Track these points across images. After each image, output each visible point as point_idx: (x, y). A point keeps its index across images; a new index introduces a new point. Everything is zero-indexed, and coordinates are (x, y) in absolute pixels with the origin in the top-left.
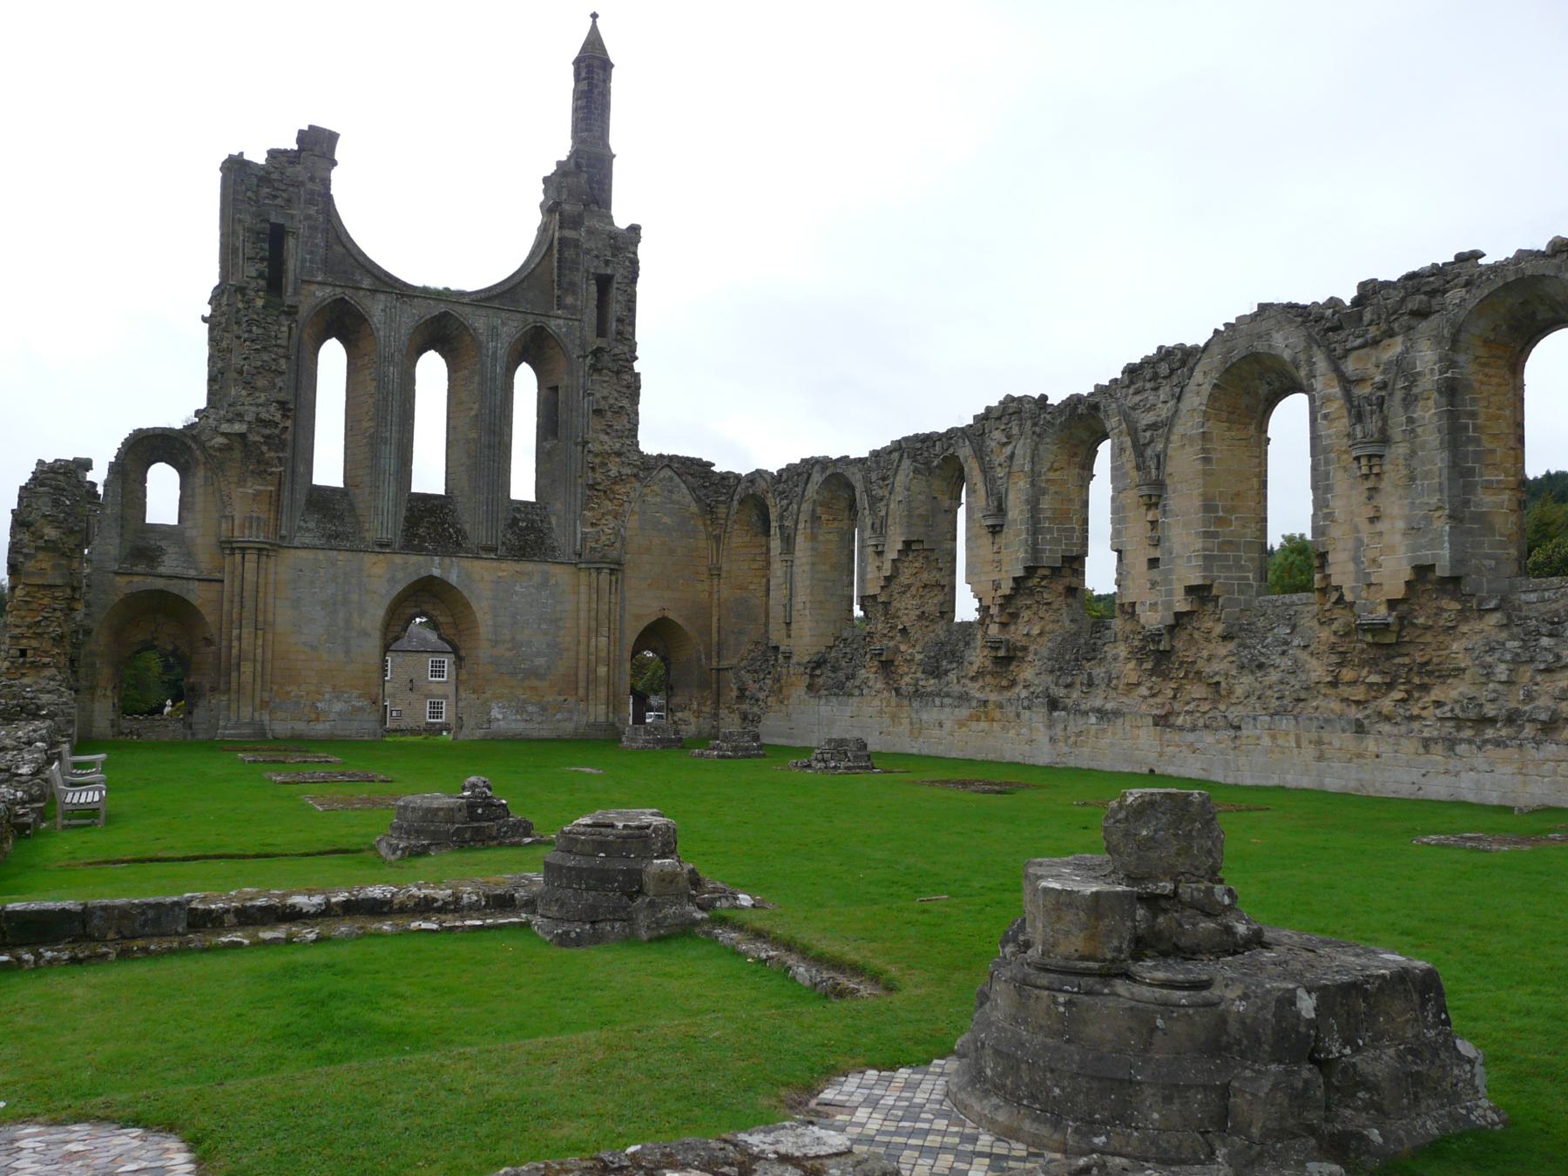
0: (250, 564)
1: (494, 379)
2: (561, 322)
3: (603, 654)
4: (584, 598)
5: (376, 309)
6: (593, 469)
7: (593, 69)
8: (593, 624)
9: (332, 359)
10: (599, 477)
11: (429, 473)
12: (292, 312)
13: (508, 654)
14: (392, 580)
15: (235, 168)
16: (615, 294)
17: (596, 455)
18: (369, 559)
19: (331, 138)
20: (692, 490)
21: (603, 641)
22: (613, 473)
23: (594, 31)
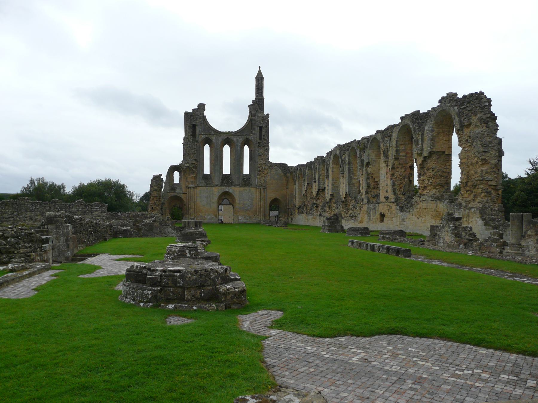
0: (192, 190)
5: (214, 138)
7: (260, 79)
9: (207, 149)
10: (260, 169)
11: (227, 170)
12: (197, 142)
14: (219, 192)
15: (186, 114)
16: (263, 130)
18: (214, 188)
19: (204, 105)
20: (282, 170)
23: (260, 70)
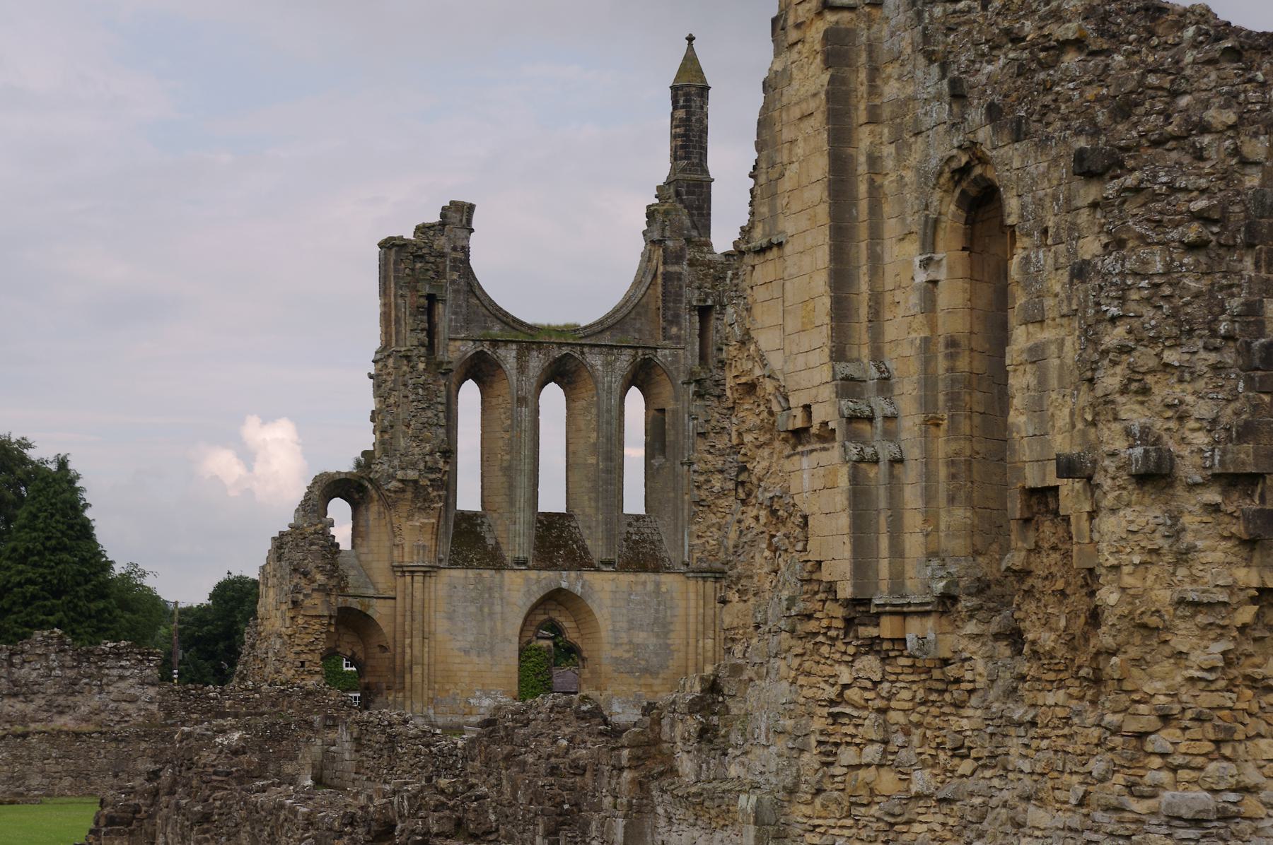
1: (609, 411)
2: (667, 352)
3: (710, 654)
4: (692, 603)
5: (508, 356)
6: (698, 487)
8: (700, 628)
13: (626, 655)
15: (390, 246)
17: (702, 474)
21: (710, 642)
22: (717, 486)
